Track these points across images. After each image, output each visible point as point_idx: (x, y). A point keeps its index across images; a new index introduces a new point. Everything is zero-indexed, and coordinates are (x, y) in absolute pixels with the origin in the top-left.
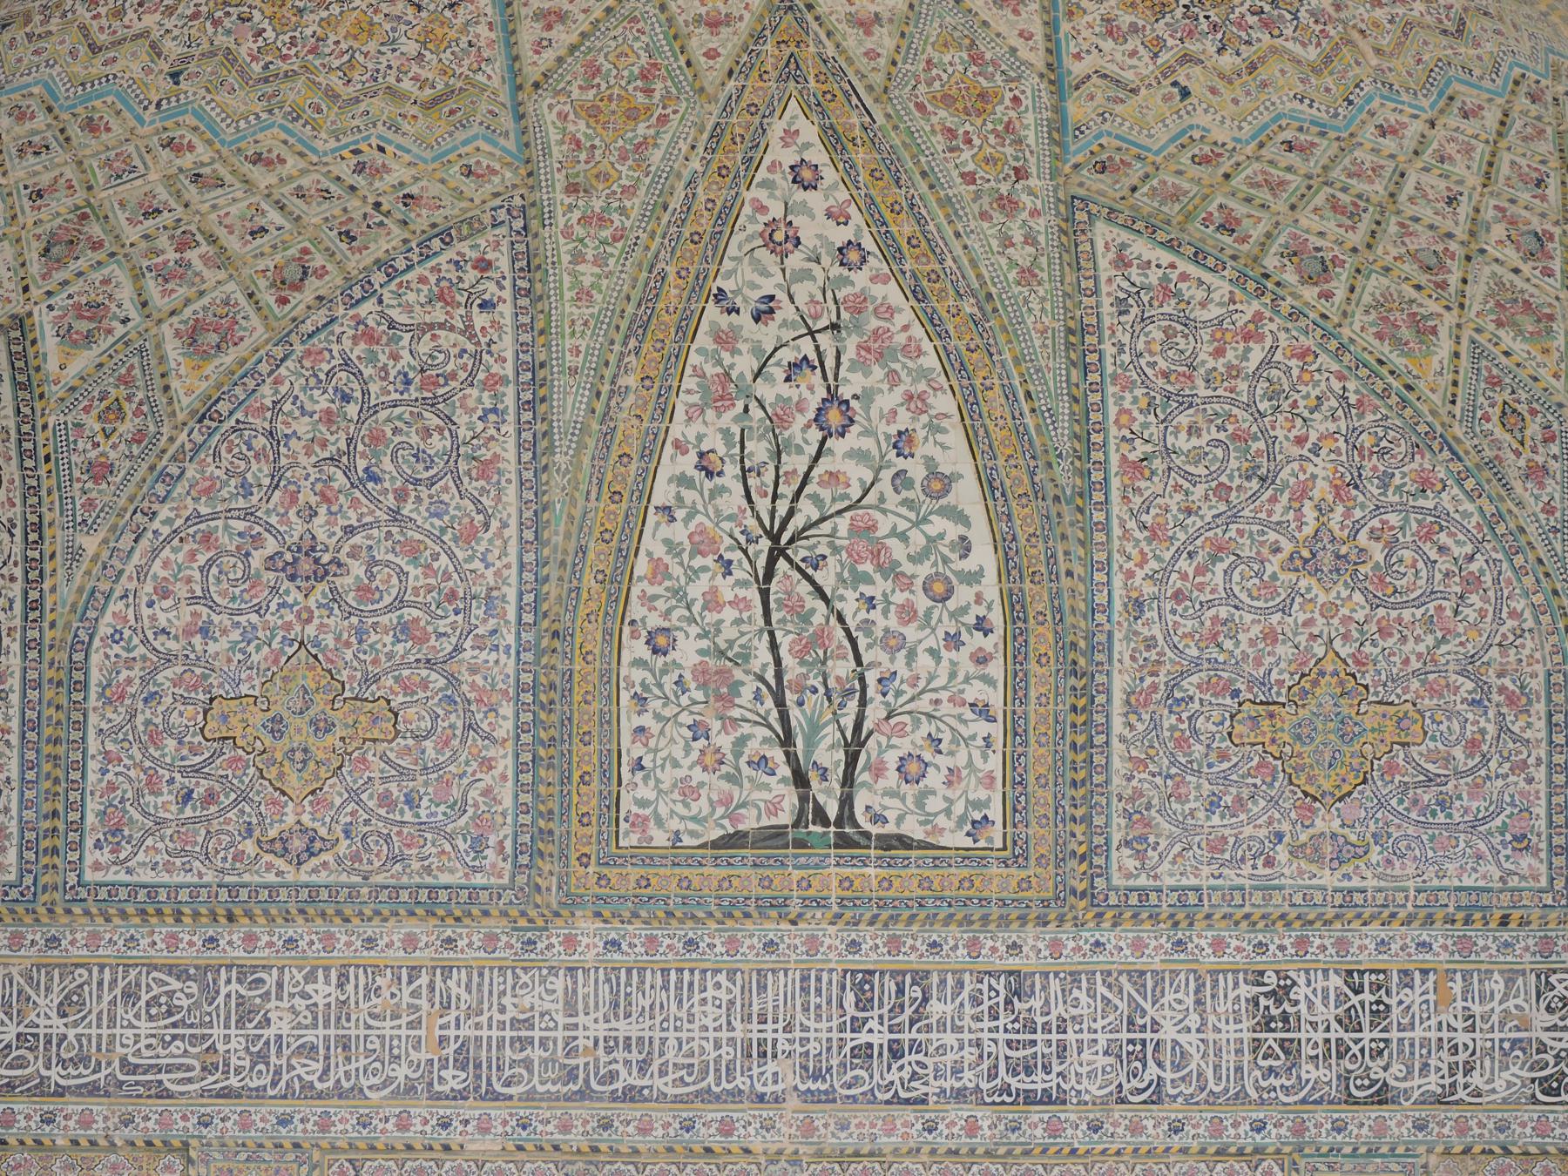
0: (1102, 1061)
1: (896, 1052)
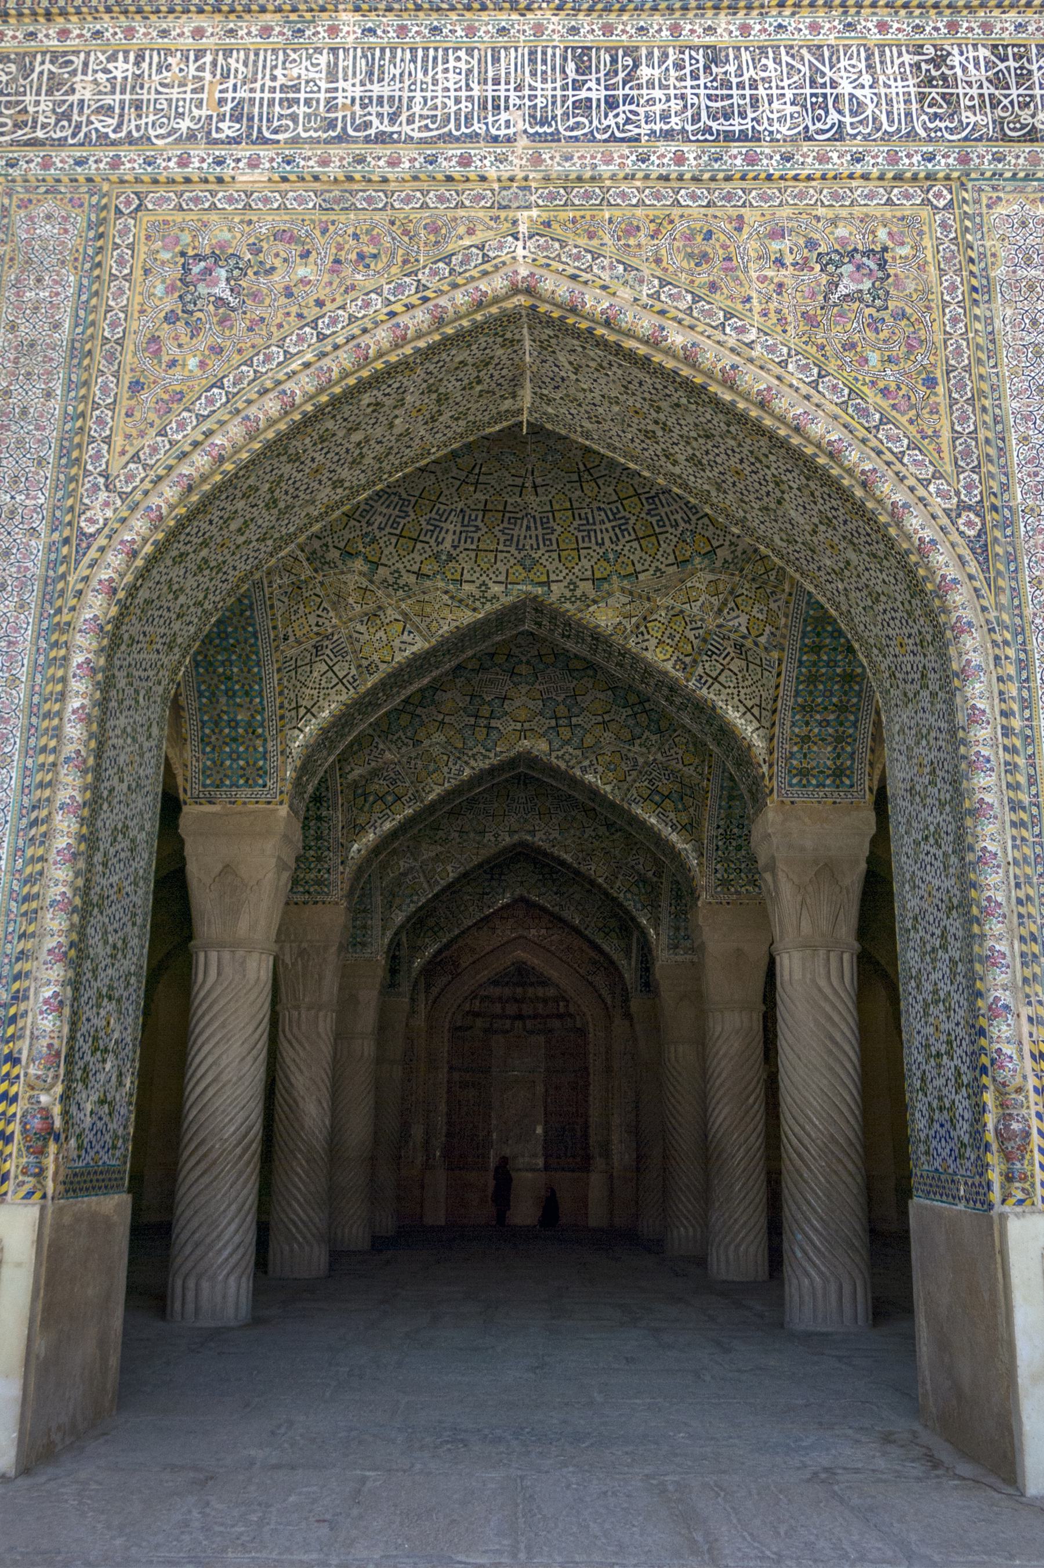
0: (789, 109)
1: (611, 104)
